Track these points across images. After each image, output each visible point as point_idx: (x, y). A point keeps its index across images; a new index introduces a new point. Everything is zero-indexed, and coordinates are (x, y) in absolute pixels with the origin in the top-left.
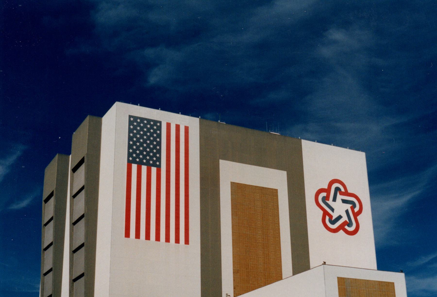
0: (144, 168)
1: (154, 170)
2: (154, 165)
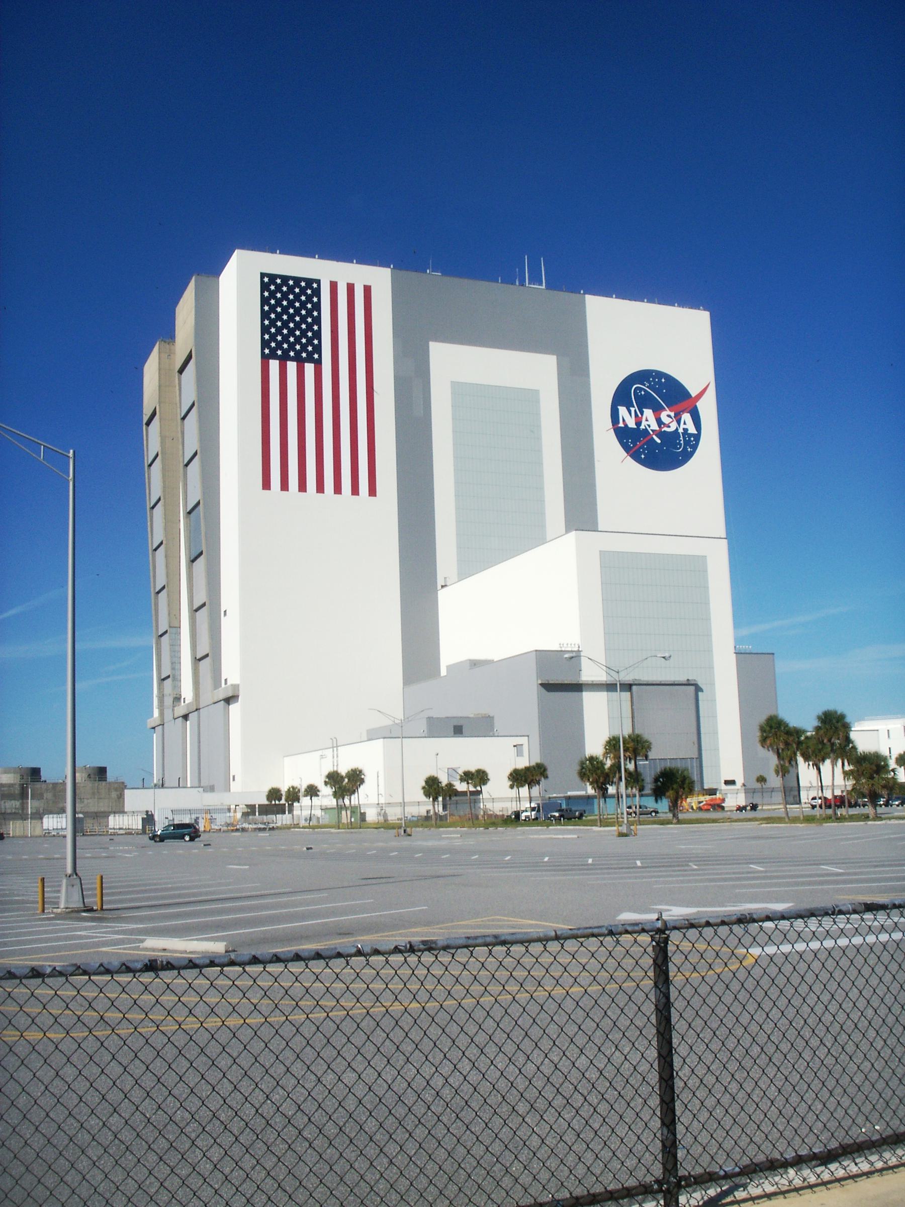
0: (292, 366)
1: (309, 368)
2: (310, 359)
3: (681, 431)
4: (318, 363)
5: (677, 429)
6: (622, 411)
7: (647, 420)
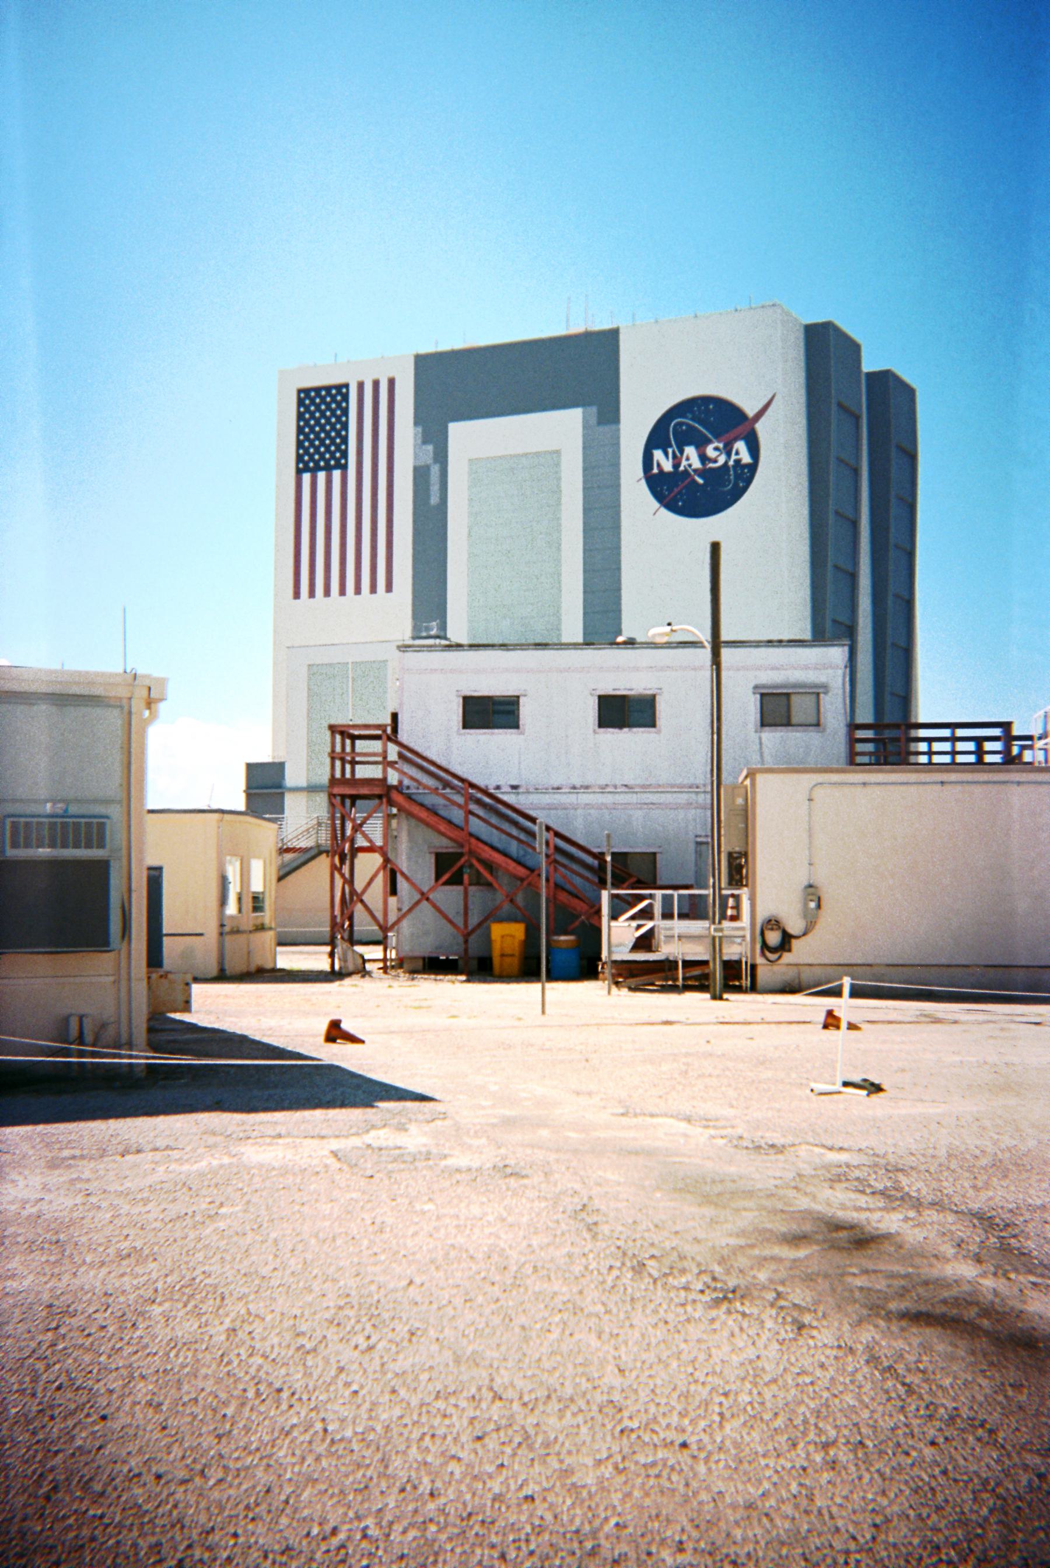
0: (321, 476)
1: (337, 474)
3: (731, 463)
4: (344, 468)
5: (726, 463)
6: (658, 455)
7: (688, 459)
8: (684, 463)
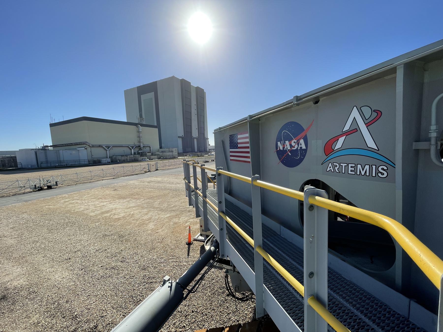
3: (299, 148)
6: (279, 143)
8: (286, 147)
